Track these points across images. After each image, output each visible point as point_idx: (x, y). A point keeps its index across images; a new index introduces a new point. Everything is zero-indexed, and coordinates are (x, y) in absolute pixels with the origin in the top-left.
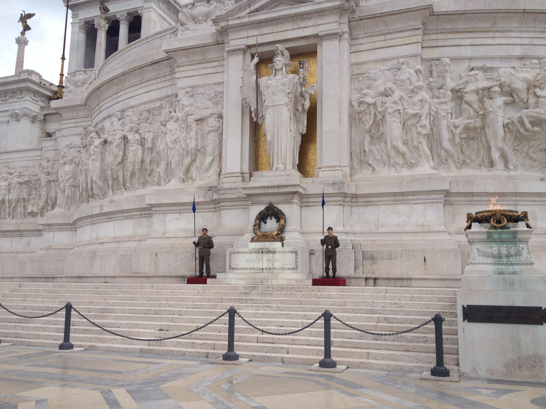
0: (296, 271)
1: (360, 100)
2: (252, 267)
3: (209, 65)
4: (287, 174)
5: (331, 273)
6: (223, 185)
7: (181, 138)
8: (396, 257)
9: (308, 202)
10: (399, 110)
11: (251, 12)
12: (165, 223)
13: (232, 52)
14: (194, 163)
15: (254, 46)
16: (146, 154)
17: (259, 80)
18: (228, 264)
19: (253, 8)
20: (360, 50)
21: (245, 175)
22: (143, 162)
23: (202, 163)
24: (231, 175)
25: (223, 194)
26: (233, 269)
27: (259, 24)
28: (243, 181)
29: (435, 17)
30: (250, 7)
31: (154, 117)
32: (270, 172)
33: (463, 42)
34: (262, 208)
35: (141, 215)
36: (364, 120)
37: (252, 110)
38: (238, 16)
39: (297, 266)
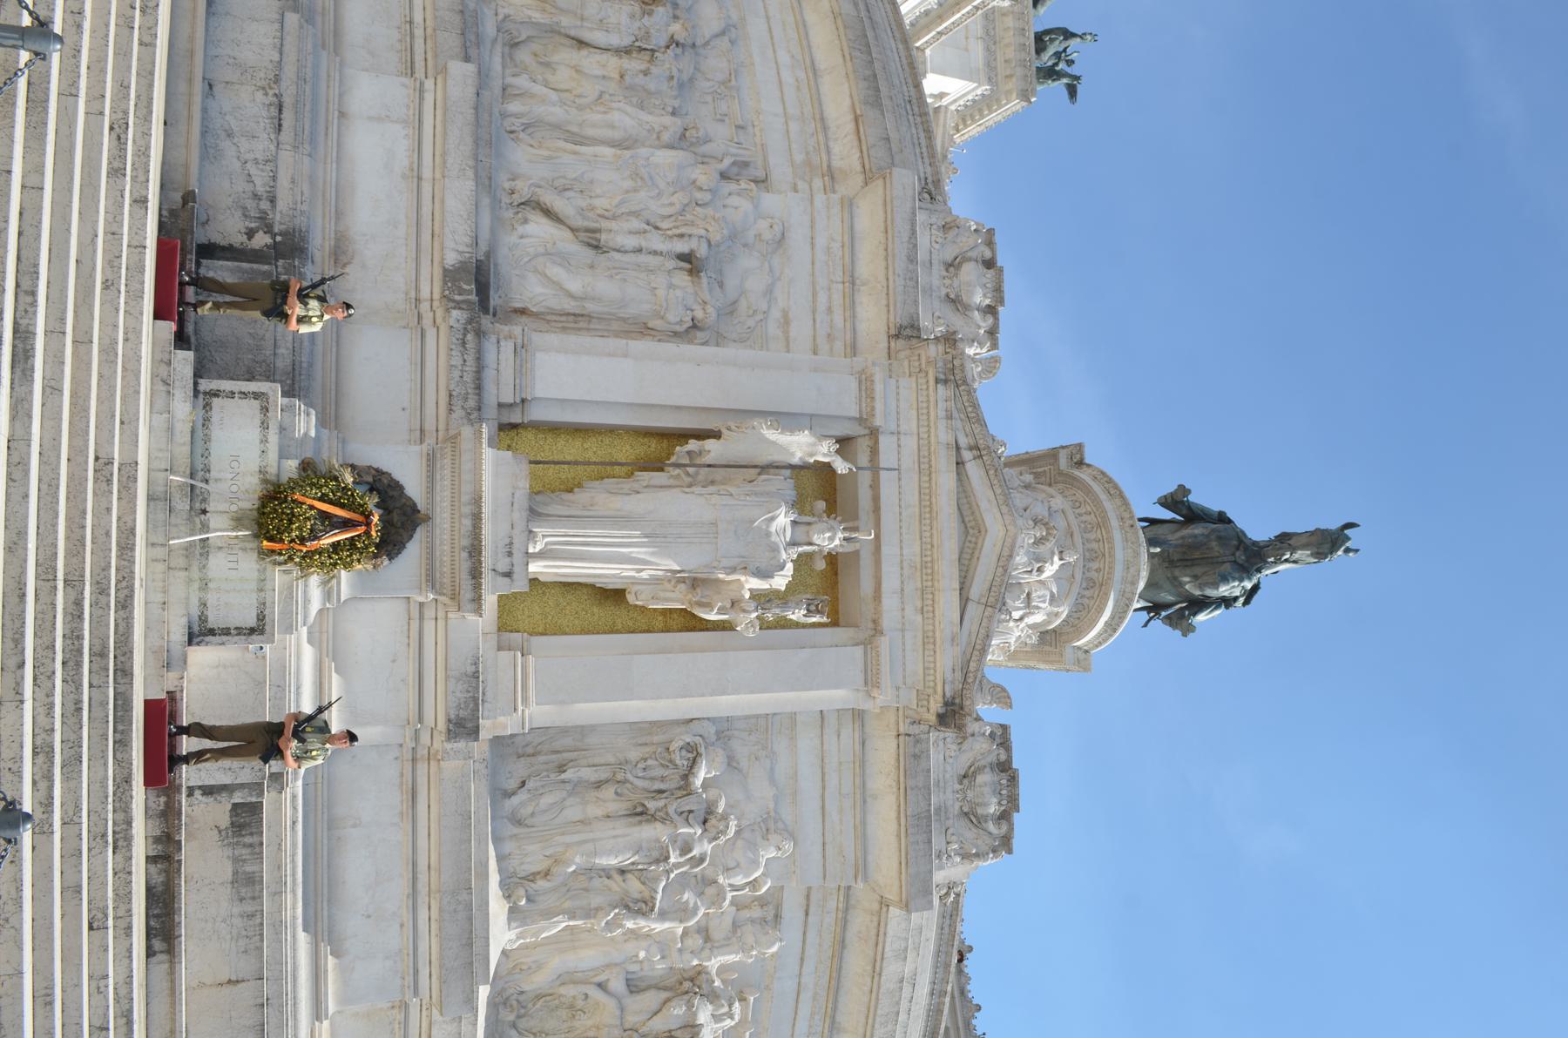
0: (196, 629)
1: (702, 750)
2: (214, 474)
3: (837, 299)
4: (516, 569)
5: (187, 744)
6: (493, 339)
7: (643, 194)
8: (241, 900)
9: (421, 618)
10: (667, 858)
11: (958, 448)
12: (379, 119)
13: (865, 384)
14: (568, 234)
15: (874, 451)
16: (605, 57)
17: (788, 472)
18: (226, 385)
19: (967, 455)
20: (826, 731)
21: (518, 410)
22: (581, 43)
23: (564, 260)
24: (522, 368)
25: (464, 343)
26: (207, 407)
27: (926, 470)
28: (500, 405)
29: (876, 906)
30: (971, 448)
31: (709, 98)
32: (525, 514)
33: (809, 967)
34: (414, 488)
35: (411, 22)
36: (650, 762)
37: (710, 444)
38: (955, 414)
39: (212, 632)
